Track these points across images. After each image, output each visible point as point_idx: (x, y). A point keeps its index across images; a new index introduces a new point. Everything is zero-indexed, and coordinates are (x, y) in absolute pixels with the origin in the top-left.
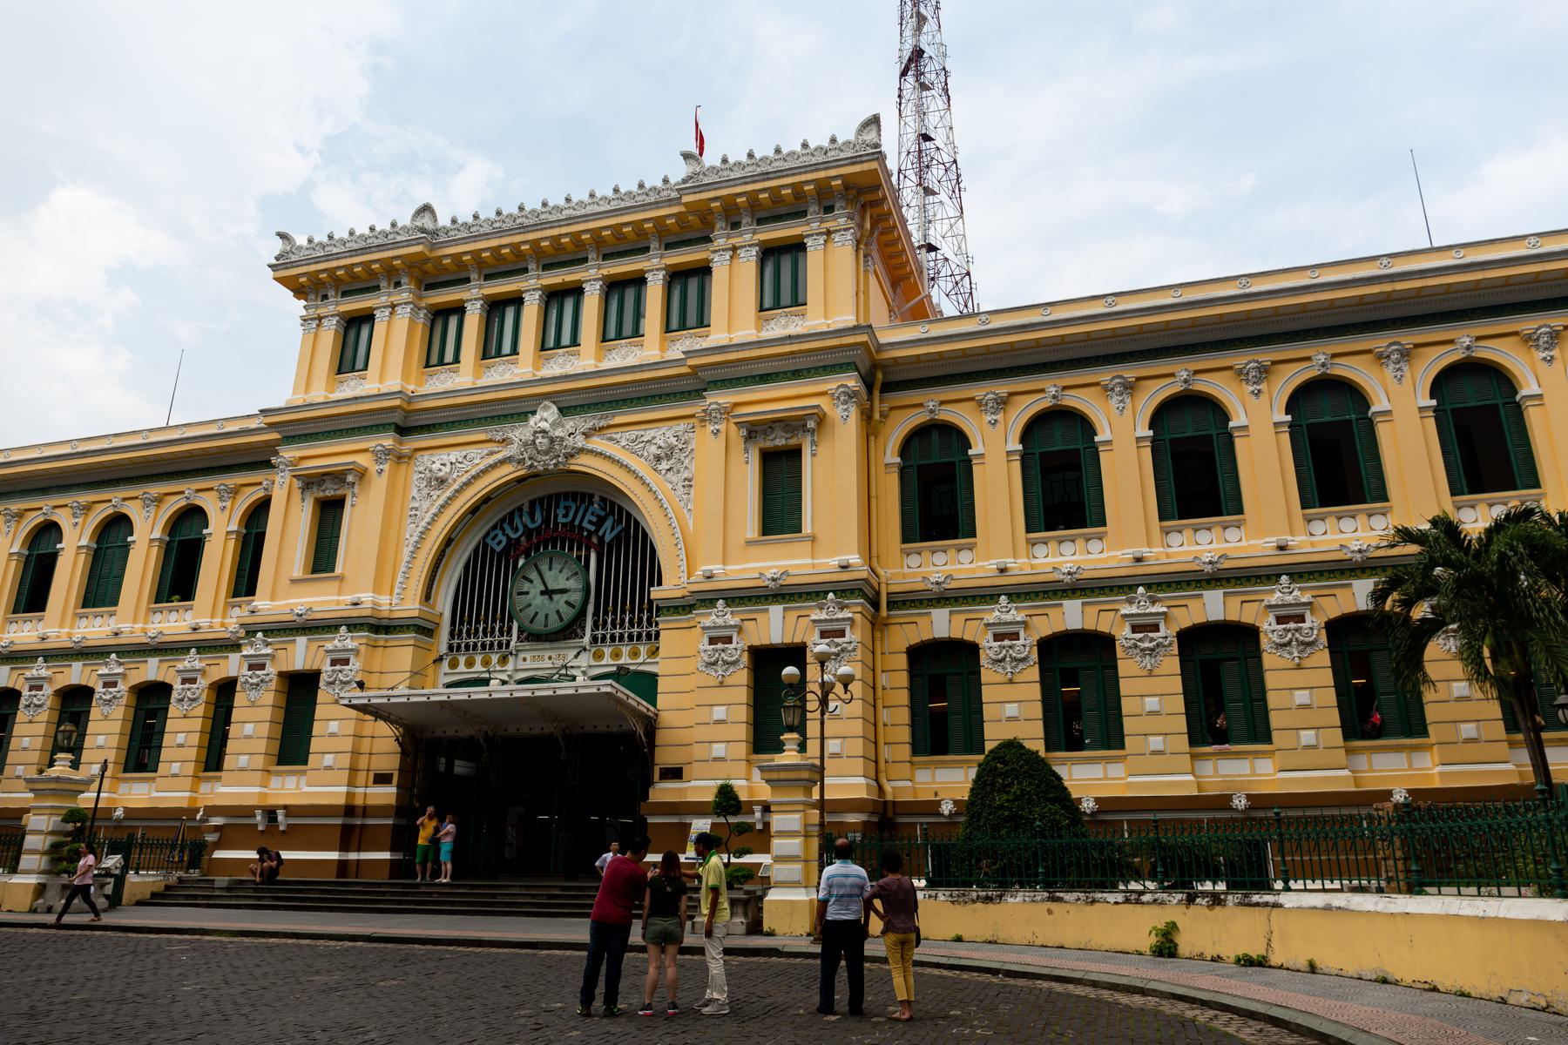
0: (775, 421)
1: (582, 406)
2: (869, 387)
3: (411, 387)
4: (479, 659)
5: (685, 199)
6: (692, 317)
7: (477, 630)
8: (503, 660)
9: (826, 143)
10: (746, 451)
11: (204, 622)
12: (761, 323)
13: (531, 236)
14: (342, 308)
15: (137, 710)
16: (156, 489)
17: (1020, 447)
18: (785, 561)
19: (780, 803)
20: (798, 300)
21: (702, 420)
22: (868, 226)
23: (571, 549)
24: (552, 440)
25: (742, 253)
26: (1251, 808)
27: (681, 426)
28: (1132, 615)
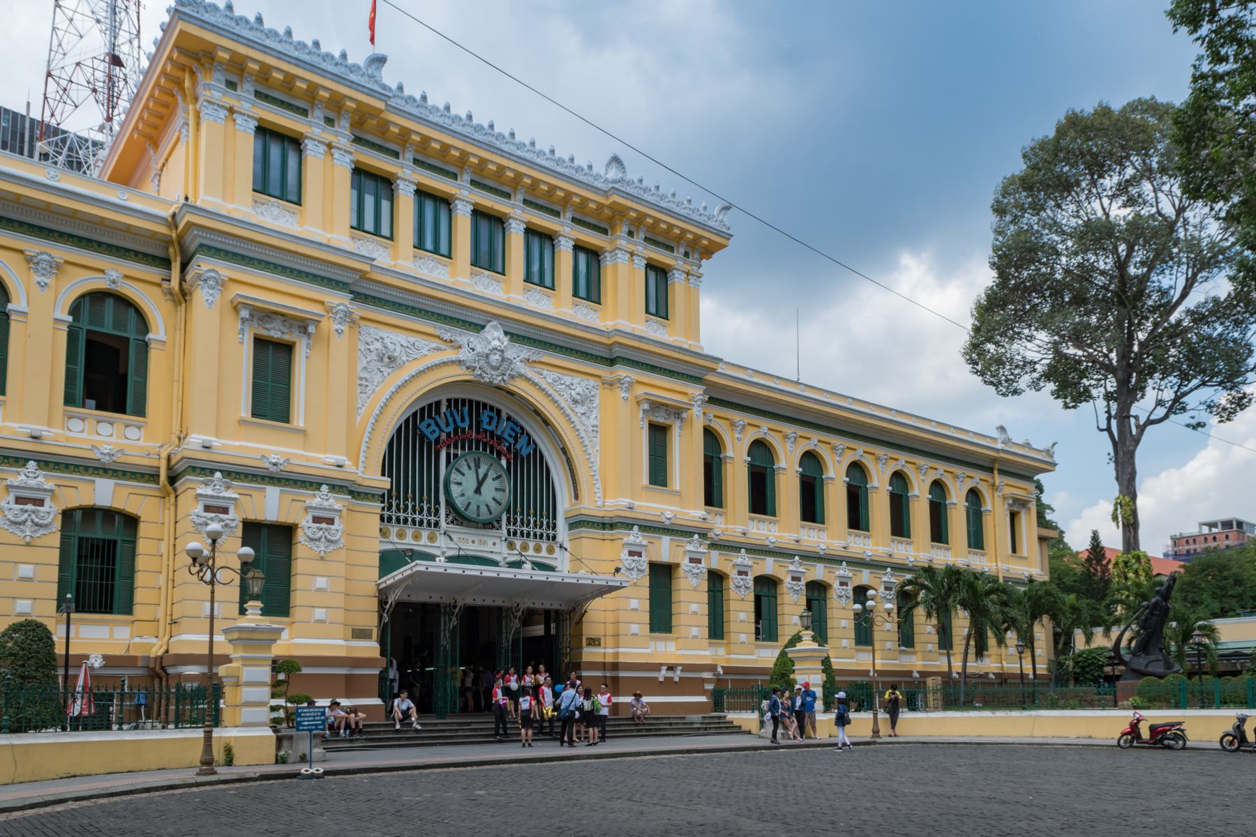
0: (663, 405)
1: (524, 337)
26: (105, 666)
27: (592, 382)
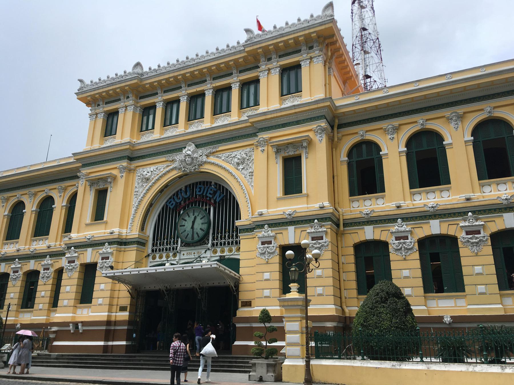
0: (288, 144)
2: (332, 127)
3: (135, 140)
4: (164, 255)
5: (247, 49)
6: (252, 103)
7: (164, 242)
8: (175, 255)
9: (308, 18)
10: (276, 158)
11: (52, 244)
12: (281, 102)
13: (182, 72)
14: (106, 109)
15: (26, 282)
16: (34, 190)
17: (406, 149)
18: (296, 206)
19: (289, 317)
20: (298, 90)
21: (257, 146)
22: (330, 54)
23: (202, 206)
24: (193, 159)
25: (272, 71)
27: (248, 149)
28: (466, 226)
